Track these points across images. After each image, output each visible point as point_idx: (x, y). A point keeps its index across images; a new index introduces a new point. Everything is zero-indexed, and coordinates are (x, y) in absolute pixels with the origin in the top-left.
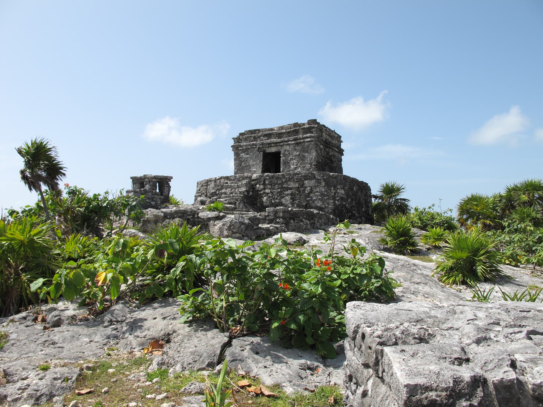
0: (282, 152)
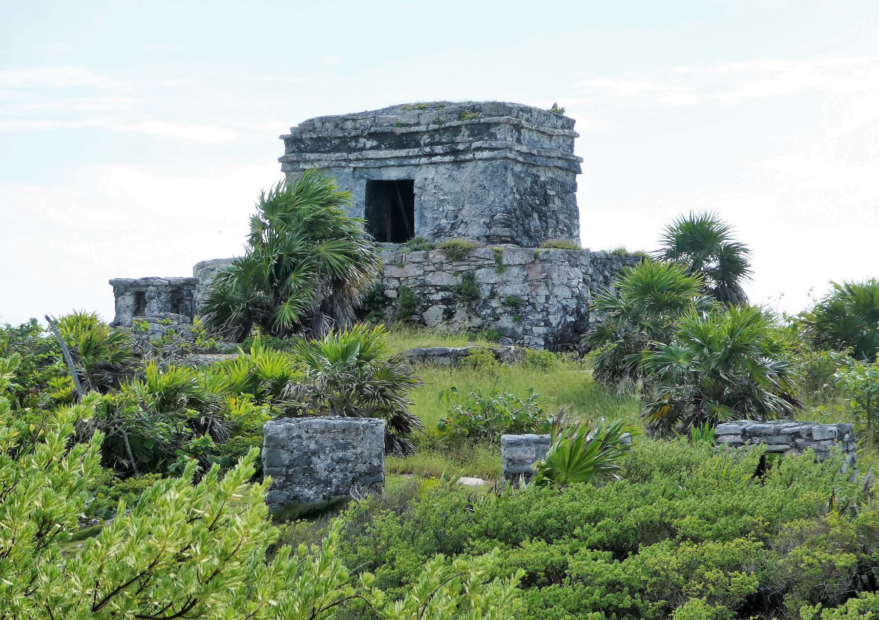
0: (417, 182)
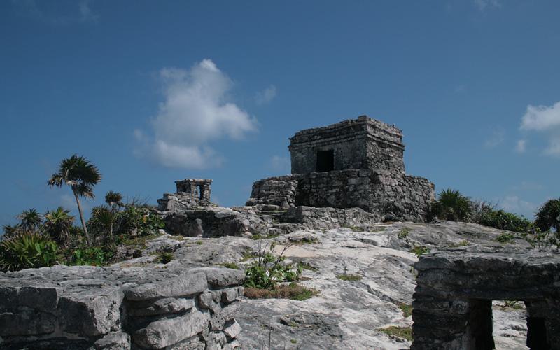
0: (336, 150)
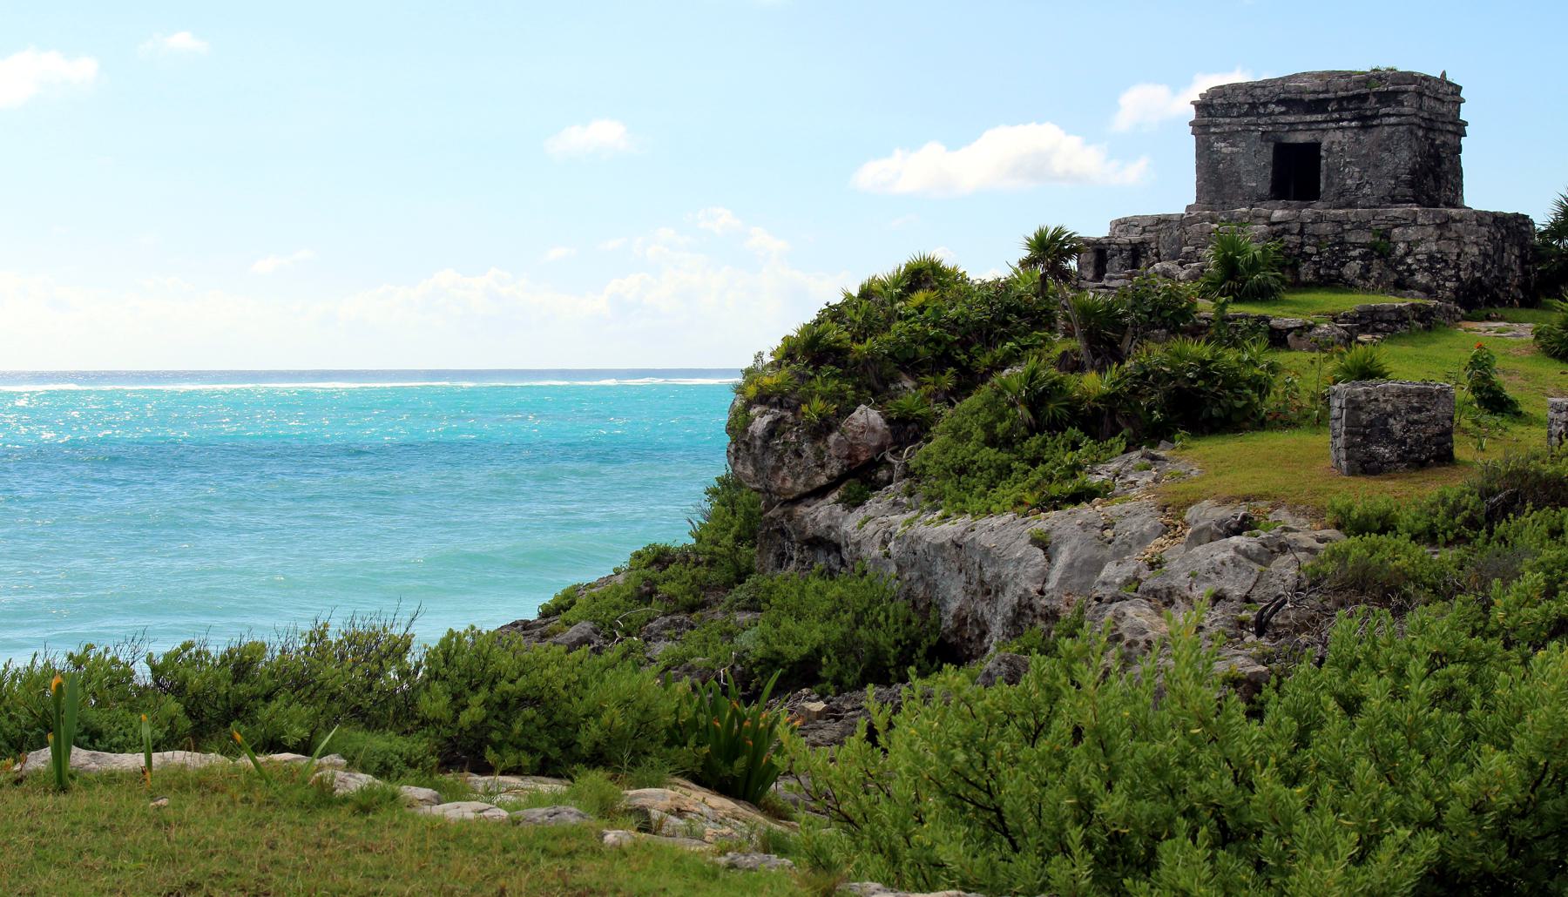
0: (1324, 145)
